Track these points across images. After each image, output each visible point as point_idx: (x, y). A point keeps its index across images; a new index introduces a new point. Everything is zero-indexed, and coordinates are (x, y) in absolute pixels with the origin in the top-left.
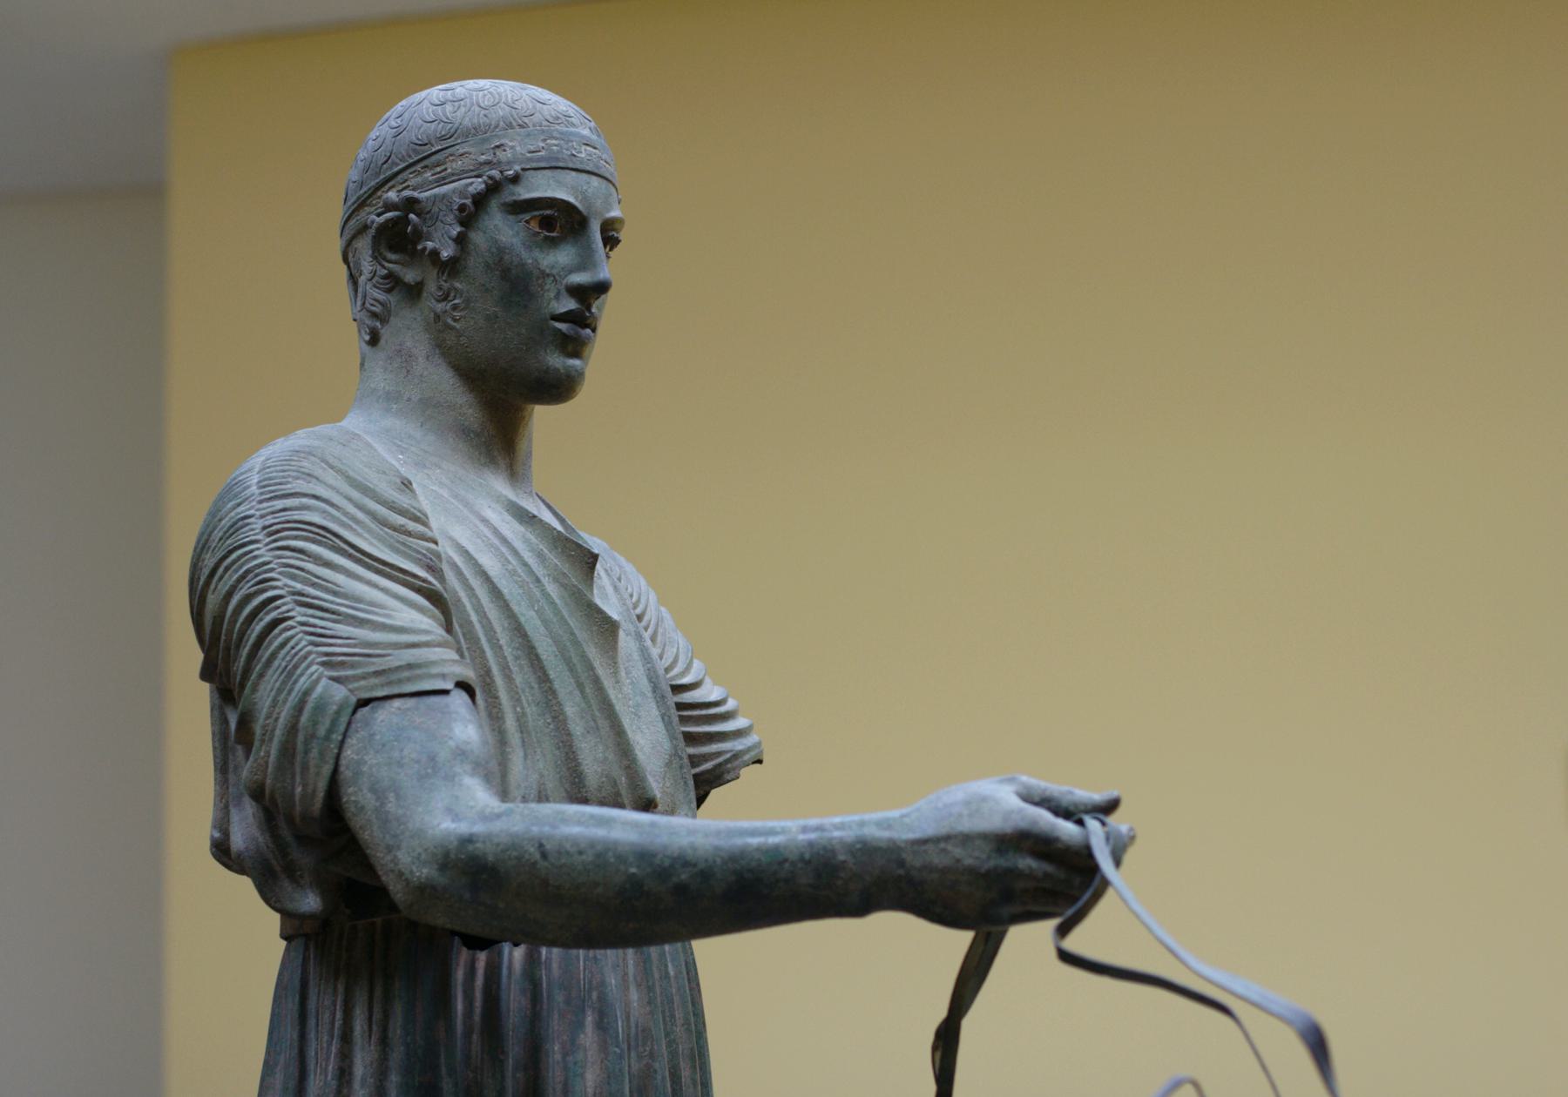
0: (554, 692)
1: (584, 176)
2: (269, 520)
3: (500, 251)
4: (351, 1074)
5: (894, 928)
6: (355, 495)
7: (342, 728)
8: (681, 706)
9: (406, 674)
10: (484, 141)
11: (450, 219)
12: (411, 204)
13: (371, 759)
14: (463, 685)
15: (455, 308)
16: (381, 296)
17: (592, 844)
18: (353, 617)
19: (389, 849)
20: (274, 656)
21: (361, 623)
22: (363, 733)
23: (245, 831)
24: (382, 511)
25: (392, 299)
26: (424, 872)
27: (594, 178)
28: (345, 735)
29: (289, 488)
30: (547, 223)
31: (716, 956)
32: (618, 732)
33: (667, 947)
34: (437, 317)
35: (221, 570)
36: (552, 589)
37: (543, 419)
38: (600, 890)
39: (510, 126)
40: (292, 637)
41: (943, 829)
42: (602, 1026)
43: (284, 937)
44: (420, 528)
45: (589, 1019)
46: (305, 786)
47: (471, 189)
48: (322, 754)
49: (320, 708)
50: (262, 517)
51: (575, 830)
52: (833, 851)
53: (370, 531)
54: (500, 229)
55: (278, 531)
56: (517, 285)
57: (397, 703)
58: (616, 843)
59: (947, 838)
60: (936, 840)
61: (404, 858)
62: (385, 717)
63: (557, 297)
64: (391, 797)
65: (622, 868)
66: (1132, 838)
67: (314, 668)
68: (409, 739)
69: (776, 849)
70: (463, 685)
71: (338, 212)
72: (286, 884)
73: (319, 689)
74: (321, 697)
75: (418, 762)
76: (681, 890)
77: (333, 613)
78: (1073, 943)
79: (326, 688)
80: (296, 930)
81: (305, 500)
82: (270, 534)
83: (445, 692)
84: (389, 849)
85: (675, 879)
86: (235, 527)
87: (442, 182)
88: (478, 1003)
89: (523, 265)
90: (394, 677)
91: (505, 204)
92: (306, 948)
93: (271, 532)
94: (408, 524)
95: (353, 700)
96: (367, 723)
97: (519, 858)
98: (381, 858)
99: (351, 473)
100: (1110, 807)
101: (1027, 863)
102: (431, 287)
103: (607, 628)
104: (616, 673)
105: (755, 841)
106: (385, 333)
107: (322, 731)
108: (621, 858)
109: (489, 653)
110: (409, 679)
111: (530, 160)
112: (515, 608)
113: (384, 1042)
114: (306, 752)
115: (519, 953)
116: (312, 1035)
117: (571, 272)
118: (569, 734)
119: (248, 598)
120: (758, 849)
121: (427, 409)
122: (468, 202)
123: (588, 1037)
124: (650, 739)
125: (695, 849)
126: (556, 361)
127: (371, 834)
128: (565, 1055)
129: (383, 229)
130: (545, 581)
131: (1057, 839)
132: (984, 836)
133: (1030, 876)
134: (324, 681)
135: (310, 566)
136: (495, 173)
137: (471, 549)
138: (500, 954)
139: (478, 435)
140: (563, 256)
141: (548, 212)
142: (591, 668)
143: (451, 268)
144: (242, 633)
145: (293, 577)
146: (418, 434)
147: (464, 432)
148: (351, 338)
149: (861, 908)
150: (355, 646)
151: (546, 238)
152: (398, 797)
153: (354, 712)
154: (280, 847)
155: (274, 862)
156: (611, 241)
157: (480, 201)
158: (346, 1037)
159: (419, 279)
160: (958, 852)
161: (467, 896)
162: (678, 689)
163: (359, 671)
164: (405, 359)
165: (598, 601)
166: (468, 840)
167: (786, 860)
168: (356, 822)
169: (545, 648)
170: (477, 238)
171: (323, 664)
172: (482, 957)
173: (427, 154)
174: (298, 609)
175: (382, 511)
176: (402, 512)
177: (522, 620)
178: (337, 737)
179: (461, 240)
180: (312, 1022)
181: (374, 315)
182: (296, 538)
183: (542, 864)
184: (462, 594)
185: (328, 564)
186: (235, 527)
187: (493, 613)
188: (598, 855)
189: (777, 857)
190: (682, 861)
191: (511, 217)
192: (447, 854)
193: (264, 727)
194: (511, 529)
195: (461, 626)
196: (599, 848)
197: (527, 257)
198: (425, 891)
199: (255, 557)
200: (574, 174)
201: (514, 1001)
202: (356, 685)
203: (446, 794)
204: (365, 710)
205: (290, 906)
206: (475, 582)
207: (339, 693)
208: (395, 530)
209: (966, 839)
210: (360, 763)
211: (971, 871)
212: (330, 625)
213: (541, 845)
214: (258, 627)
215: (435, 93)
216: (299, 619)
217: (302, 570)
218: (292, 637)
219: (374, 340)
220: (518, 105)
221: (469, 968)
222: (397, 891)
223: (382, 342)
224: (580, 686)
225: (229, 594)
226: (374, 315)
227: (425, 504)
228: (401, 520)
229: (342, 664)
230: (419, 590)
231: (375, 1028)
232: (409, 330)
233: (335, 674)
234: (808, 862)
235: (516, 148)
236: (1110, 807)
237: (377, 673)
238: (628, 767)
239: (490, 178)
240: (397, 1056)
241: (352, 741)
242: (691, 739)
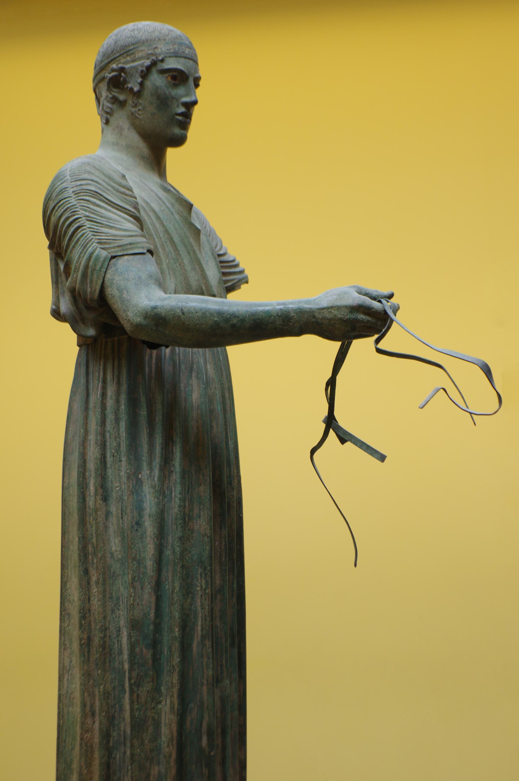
0: (180, 255)
1: (187, 60)
2: (75, 189)
3: (157, 88)
4: (106, 395)
5: (310, 340)
6: (107, 180)
7: (106, 267)
8: (221, 262)
9: (129, 247)
10: (150, 45)
11: (137, 75)
12: (122, 69)
13: (117, 278)
14: (150, 252)
15: (139, 110)
16: (110, 105)
17: (201, 309)
18: (108, 225)
19: (125, 311)
20: (78, 240)
21: (111, 227)
22: (113, 269)
23: (65, 307)
24: (116, 186)
25: (115, 107)
26: (138, 320)
28: (107, 269)
29: (82, 177)
30: (174, 78)
31: (234, 352)
32: (202, 270)
33: (219, 348)
34: (132, 114)
35: (57, 207)
36: (177, 217)
37: (171, 153)
38: (204, 326)
40: (85, 233)
41: (330, 305)
42: (197, 378)
43: (79, 345)
44: (130, 193)
45: (194, 375)
46: (91, 288)
47: (146, 64)
48: (98, 277)
49: (97, 259)
50: (72, 188)
51: (194, 304)
52: (289, 312)
53: (113, 194)
54: (156, 80)
55: (78, 193)
56: (163, 102)
57: (126, 257)
58: (209, 309)
59: (332, 307)
60: (328, 308)
61: (130, 314)
62: (122, 263)
63: (178, 106)
64: (125, 292)
65: (212, 318)
66: (399, 308)
67: (94, 244)
68: (131, 271)
69: (268, 312)
70: (150, 252)
71: (91, 74)
72: (82, 325)
73: (96, 252)
74: (97, 255)
75: (135, 279)
76: (233, 326)
77: (101, 224)
78: (380, 346)
79: (99, 252)
80: (84, 343)
81: (88, 182)
82: (75, 194)
83: (143, 254)
84: (125, 311)
86: (62, 191)
87: (134, 61)
88: (153, 369)
90: (125, 248)
92: (88, 349)
93: (76, 193)
94: (127, 191)
95: (110, 256)
96: (115, 265)
97: (174, 315)
98: (121, 315)
99: (105, 172)
100: (391, 296)
101: (361, 317)
102: (130, 102)
103: (197, 232)
104: (200, 249)
105: (260, 308)
106: (112, 120)
107: (98, 268)
108: (212, 315)
109: (156, 240)
110: (130, 249)
111: (167, 53)
112: (165, 223)
113: (119, 383)
114: (92, 275)
115: (168, 350)
116: (91, 381)
117: (182, 96)
118: (186, 270)
119: (68, 218)
120: (261, 312)
121: (129, 148)
122: (144, 69)
123: (194, 382)
124: (212, 273)
125: (238, 311)
126: (177, 131)
127: (117, 306)
128: (185, 388)
129: (111, 79)
130: (174, 213)
131: (373, 308)
132: (346, 307)
133: (363, 321)
134: (98, 249)
135: (91, 206)
136: (154, 58)
137: (148, 201)
138: (161, 350)
140: (180, 91)
142: (192, 246)
143: (138, 94)
144: (66, 232)
145: (85, 210)
146: (125, 158)
147: (142, 158)
148: (97, 121)
149: (299, 333)
150: (110, 236)
151: (174, 84)
152: (127, 292)
153: (110, 261)
154: (80, 312)
155: (77, 317)
156: (197, 85)
157: (149, 69)
158: (104, 382)
160: (336, 312)
161: (154, 328)
162: (219, 255)
163: (111, 246)
164: (120, 129)
165: (193, 221)
166: (155, 308)
167: (272, 316)
168: (111, 302)
169: (176, 239)
170: (148, 84)
171: (98, 243)
172: (155, 352)
173: (126, 50)
174: (87, 222)
175: (116, 186)
176: (124, 187)
177: (168, 228)
178: (104, 270)
179: (141, 84)
180: (91, 376)
181: (107, 113)
182: (86, 196)
183: (182, 316)
184: (146, 218)
185: (98, 206)
186: (62, 191)
187: (158, 225)
188: (203, 313)
189: (268, 314)
190: (234, 315)
191: (161, 76)
192: (147, 313)
193: (75, 266)
194: (162, 194)
198: (138, 327)
199: (70, 203)
200: (183, 59)
201: (168, 368)
202: (111, 251)
203: (142, 293)
204: (114, 260)
205: (83, 333)
206: (151, 214)
207: (104, 253)
209: (339, 308)
210: (113, 279)
211: (341, 319)
212: (100, 228)
213: (182, 310)
214: (72, 229)
215: (130, 26)
216: (88, 226)
217: (88, 208)
218: (85, 233)
219: (107, 122)
220: (162, 32)
221: (150, 356)
222: (127, 327)
223: (110, 123)
224: (189, 253)
225: (60, 217)
226: (107, 113)
227: (131, 184)
228: (123, 190)
229: (105, 243)
230: (131, 216)
231: (115, 378)
232: (121, 118)
233: (102, 246)
234: (280, 316)
235: (162, 49)
236: (391, 296)
237: (118, 246)
238: (205, 283)
239: (152, 60)
240: (124, 387)
241: (109, 271)
242: (224, 274)
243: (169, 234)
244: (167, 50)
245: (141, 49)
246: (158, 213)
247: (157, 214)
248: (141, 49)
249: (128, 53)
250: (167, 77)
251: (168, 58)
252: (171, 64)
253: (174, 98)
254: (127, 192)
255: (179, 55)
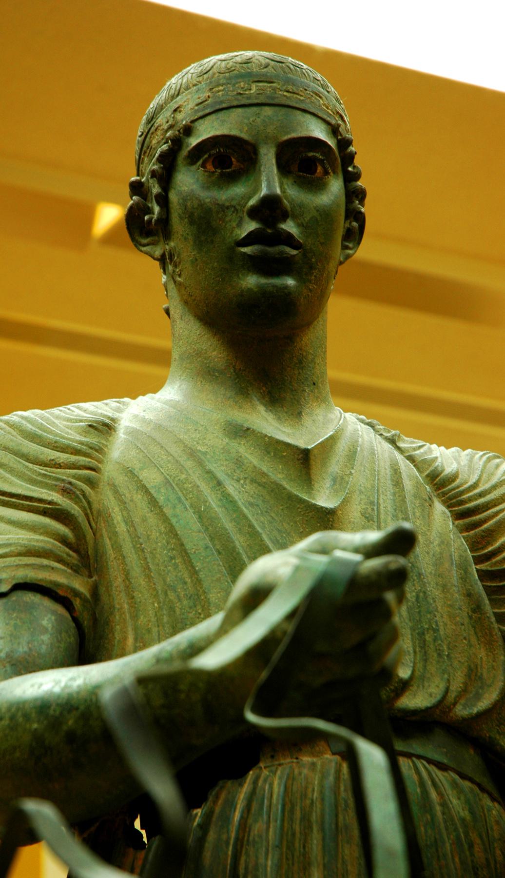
0: (199, 581)
27: (267, 109)
30: (221, 162)
38: (17, 754)
39: (187, 88)
53: (11, 471)
54: (188, 181)
63: (240, 224)
65: (28, 726)
76: (71, 737)
85: (65, 728)
89: (201, 205)
91: (185, 159)
108: (27, 717)
111: (198, 111)
112: (168, 511)
117: (250, 198)
137: (137, 466)
139: (221, 372)
141: (213, 152)
159: (162, 252)
170: (173, 197)
177: (174, 521)
187: (152, 519)
191: (194, 168)
195: (110, 539)
196: (13, 710)
197: (208, 196)
200: (240, 110)
208: (46, 465)
230: (44, 513)
243: (176, 535)
244: (197, 105)
245: (156, 125)
246: (152, 491)
247: (150, 493)
248: (156, 125)
249: (145, 149)
250: (203, 166)
251: (200, 121)
252: (206, 131)
253: (228, 208)
254: (63, 457)
255: (224, 105)
